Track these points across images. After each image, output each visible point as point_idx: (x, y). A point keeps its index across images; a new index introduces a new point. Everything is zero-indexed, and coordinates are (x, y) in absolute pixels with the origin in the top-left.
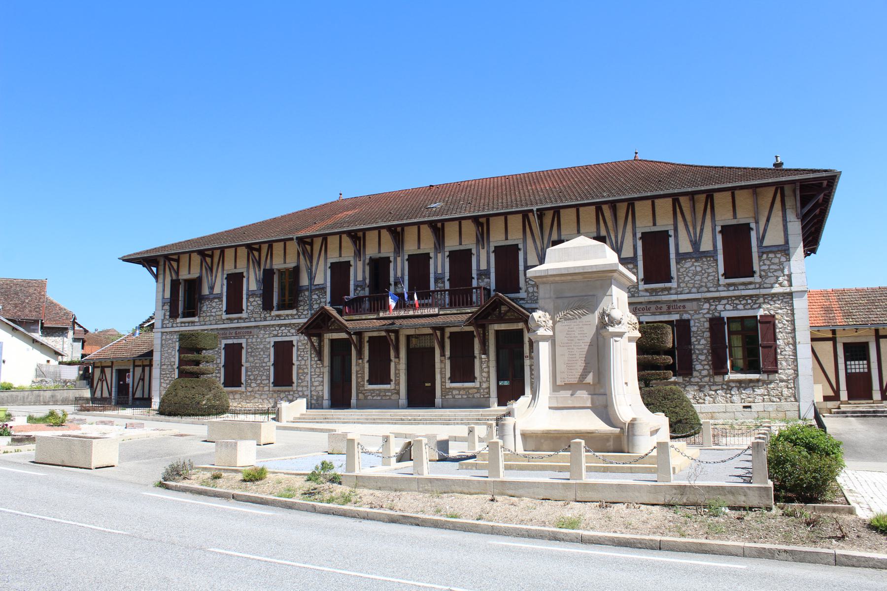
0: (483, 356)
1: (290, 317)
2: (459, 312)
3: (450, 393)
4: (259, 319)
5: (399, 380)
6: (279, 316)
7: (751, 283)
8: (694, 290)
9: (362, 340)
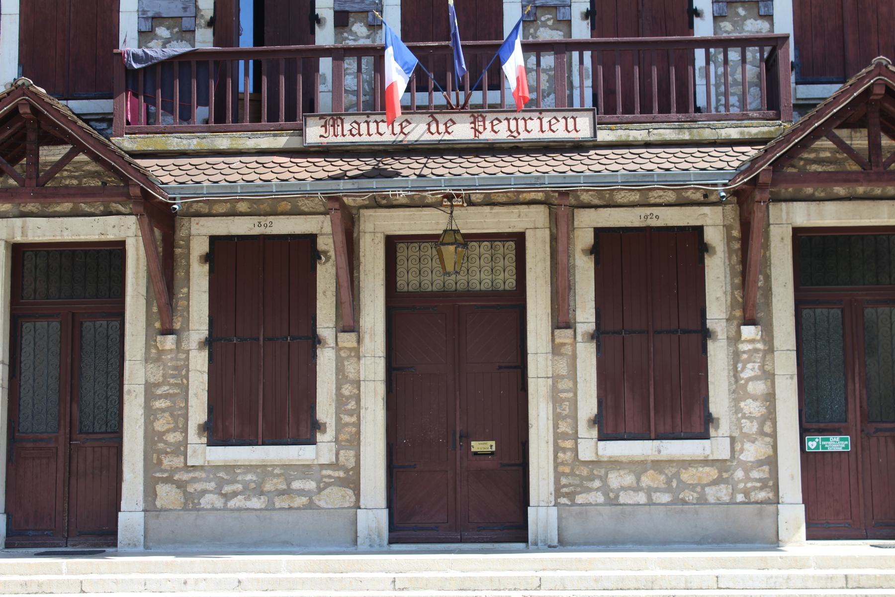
0: (748, 332)
2: (686, 136)
3: (597, 484)
5: (358, 425)
9: (178, 251)
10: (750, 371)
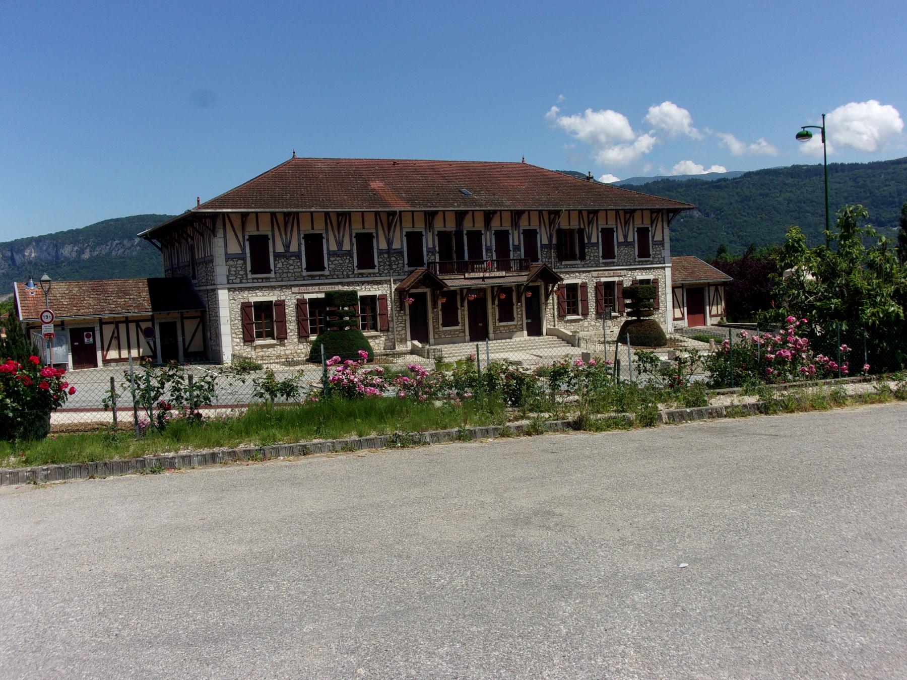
0: (519, 304)
1: (372, 275)
4: (342, 276)
6: (362, 275)
7: (649, 261)
8: (625, 264)
10: (519, 310)
